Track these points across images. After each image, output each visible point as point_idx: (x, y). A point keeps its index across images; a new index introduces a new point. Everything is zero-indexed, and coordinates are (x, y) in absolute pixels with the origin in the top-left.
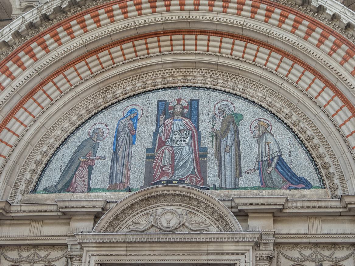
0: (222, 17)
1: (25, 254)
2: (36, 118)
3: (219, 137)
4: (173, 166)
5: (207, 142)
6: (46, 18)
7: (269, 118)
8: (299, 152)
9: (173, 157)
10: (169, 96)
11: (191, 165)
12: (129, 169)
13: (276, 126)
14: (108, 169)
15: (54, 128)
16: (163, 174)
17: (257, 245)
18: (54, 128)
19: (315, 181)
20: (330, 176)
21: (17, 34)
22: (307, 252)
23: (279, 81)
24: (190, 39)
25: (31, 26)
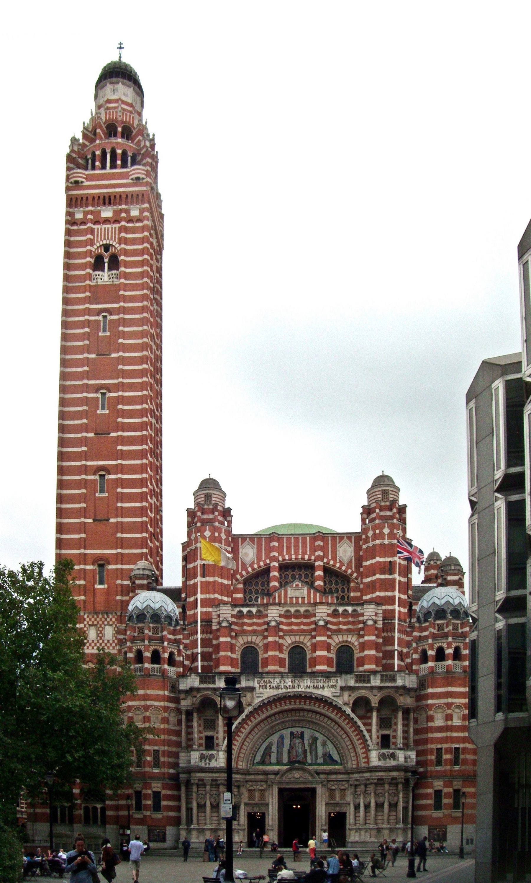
0: (313, 708)
1: (254, 783)
2: (252, 740)
3: (311, 746)
4: (297, 756)
5: (307, 747)
6: (255, 709)
7: (327, 740)
8: (335, 752)
9: (296, 752)
10: (294, 730)
11: (302, 756)
12: (282, 755)
13: (329, 743)
14: (276, 756)
15: (256, 742)
16: (294, 758)
17: (322, 783)
18: (256, 742)
19: (339, 761)
20: (344, 760)
21: (247, 716)
22: (335, 783)
23: (330, 728)
24: (302, 713)
25: (251, 712)
